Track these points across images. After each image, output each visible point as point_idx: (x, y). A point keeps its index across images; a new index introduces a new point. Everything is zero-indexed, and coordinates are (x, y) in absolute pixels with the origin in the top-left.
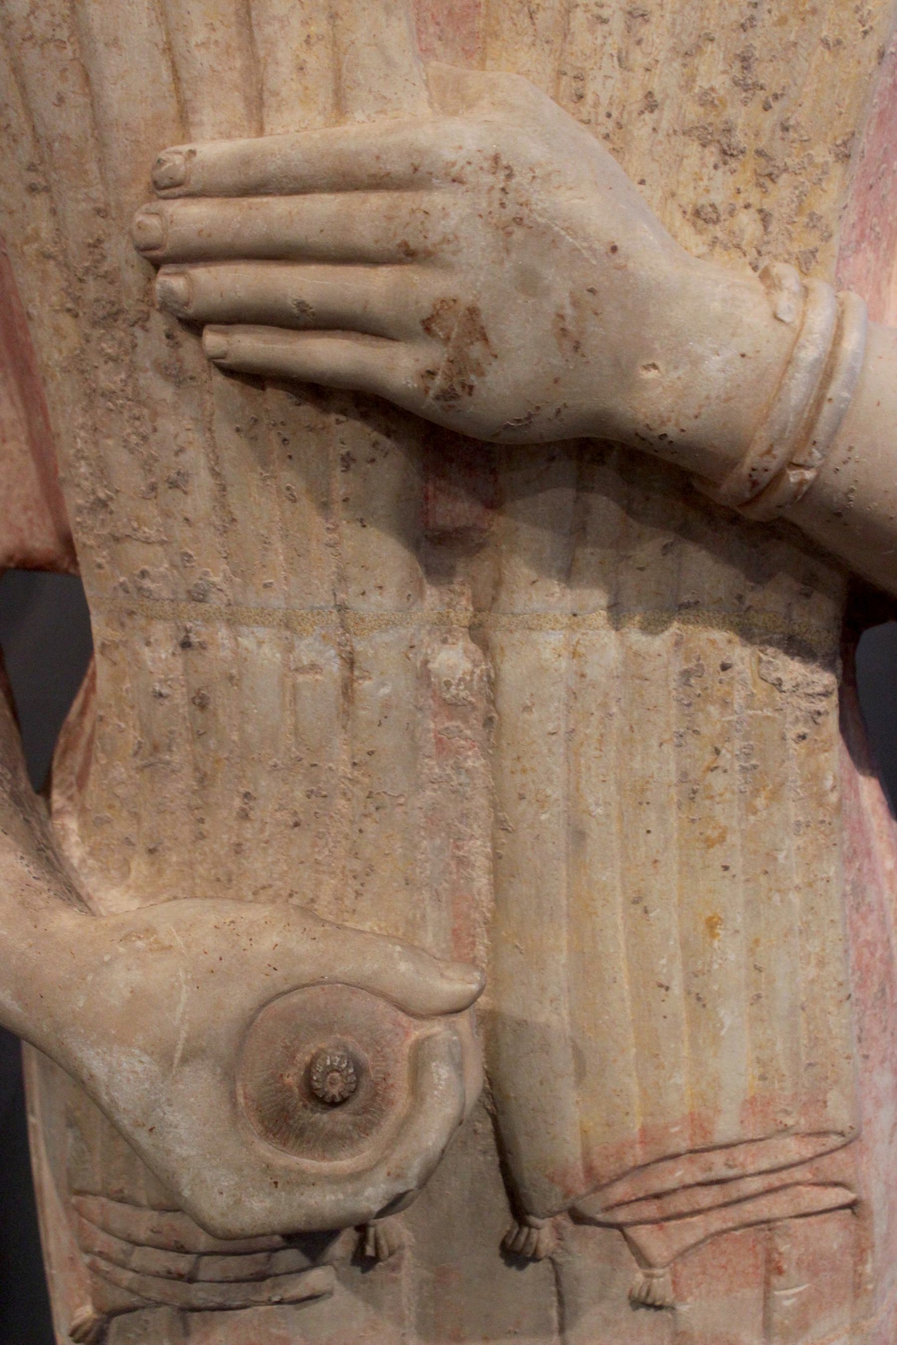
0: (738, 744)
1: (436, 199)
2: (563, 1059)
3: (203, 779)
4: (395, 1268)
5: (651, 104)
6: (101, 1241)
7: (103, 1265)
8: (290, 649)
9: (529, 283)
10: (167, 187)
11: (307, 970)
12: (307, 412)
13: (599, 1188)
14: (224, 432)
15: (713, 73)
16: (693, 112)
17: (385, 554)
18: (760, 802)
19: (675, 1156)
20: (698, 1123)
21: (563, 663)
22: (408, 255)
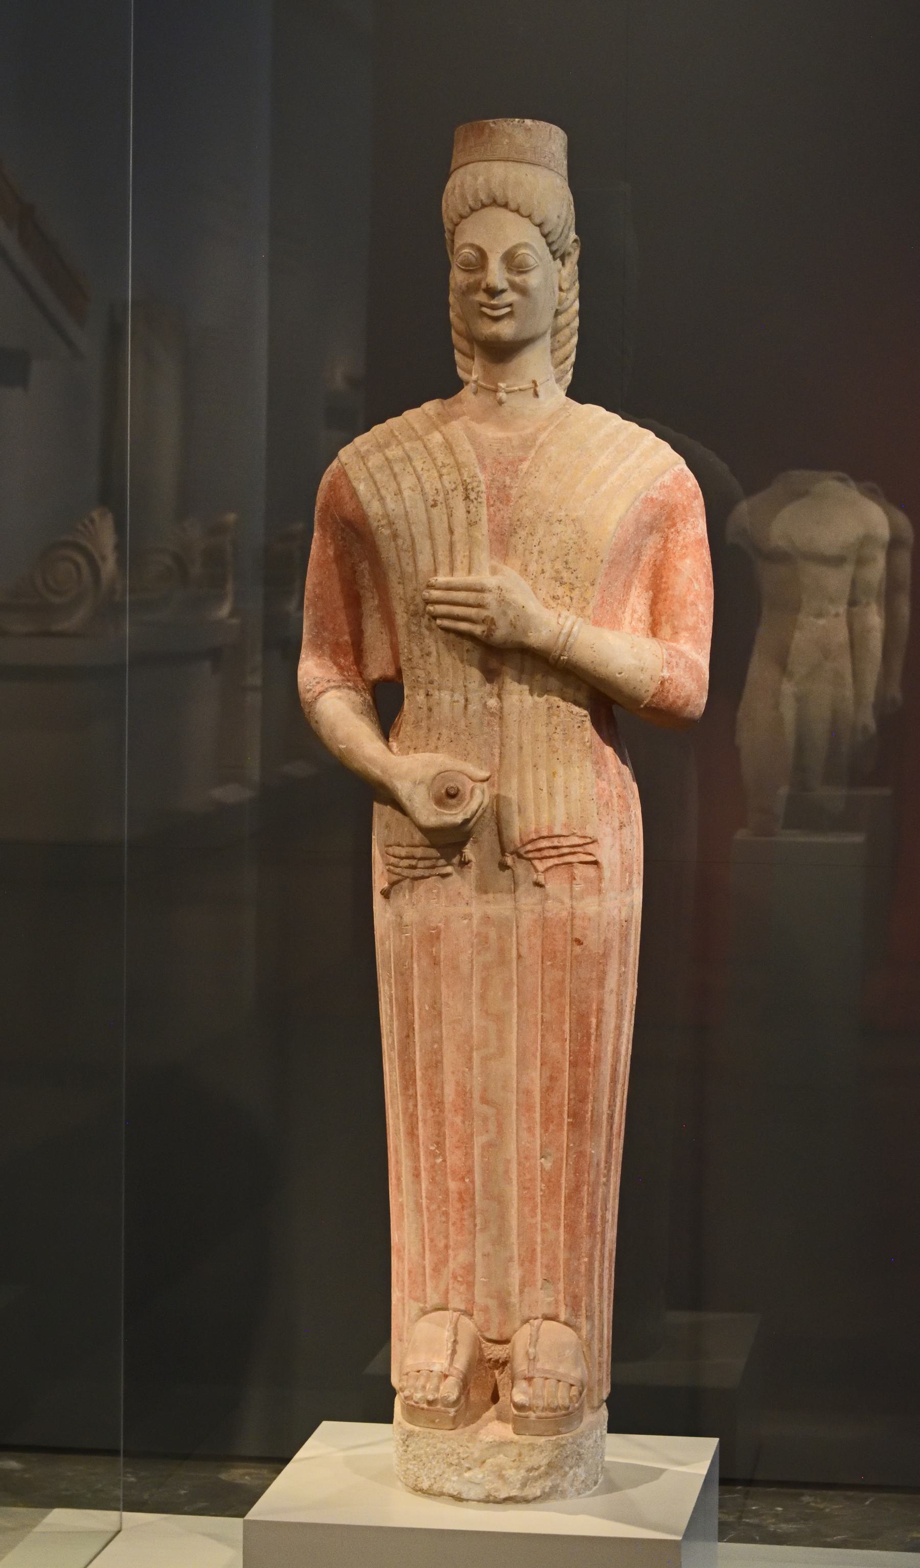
0: (562, 727)
1: (486, 595)
2: (515, 808)
3: (429, 730)
4: (470, 868)
5: (543, 572)
6: (392, 860)
7: (392, 868)
8: (452, 696)
9: (505, 613)
10: (430, 587)
11: (449, 767)
12: (458, 639)
13: (524, 845)
14: (441, 645)
15: (559, 565)
16: (554, 574)
17: (475, 674)
18: (568, 743)
19: (544, 838)
20: (550, 828)
21: (518, 703)
22: (479, 606)
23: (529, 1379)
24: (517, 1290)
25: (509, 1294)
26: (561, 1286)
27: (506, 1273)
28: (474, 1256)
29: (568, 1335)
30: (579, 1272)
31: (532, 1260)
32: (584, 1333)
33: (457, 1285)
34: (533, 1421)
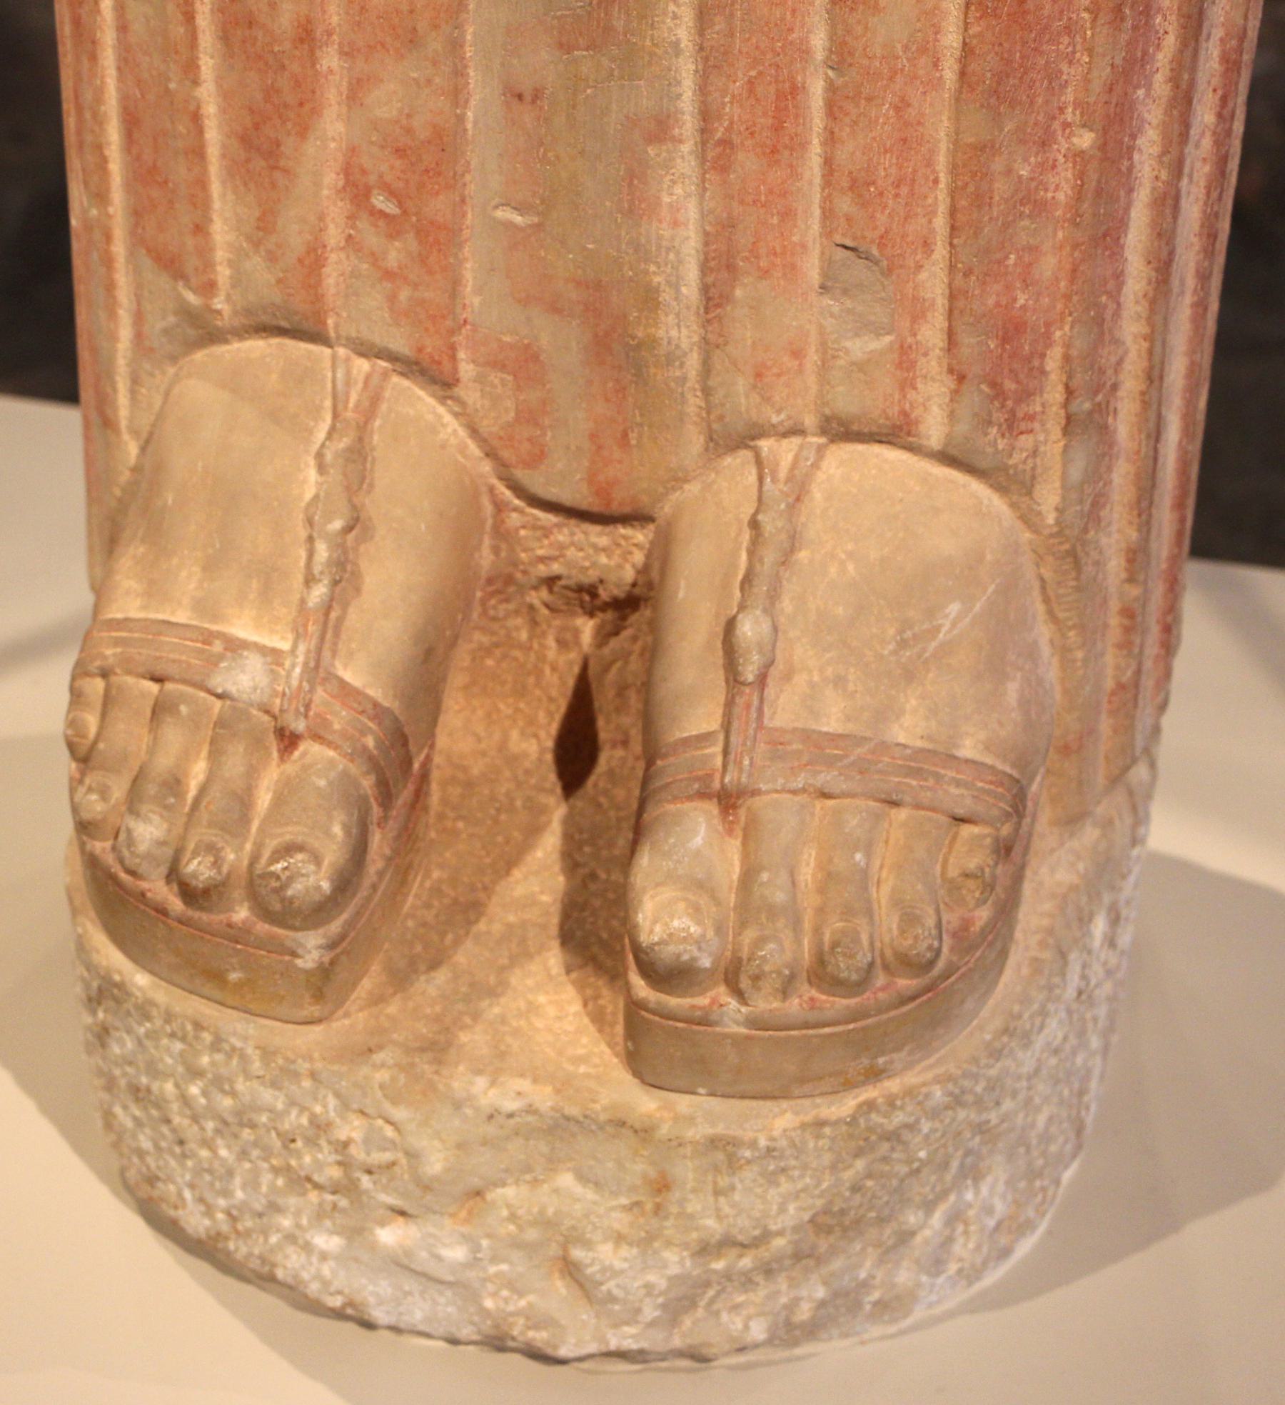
23: (728, 801)
24: (690, 288)
25: (650, 300)
26: (933, 281)
27: (634, 197)
28: (457, 95)
29: (957, 516)
30: (1041, 208)
31: (780, 144)
32: (1048, 498)
33: (371, 237)
34: (737, 1041)
